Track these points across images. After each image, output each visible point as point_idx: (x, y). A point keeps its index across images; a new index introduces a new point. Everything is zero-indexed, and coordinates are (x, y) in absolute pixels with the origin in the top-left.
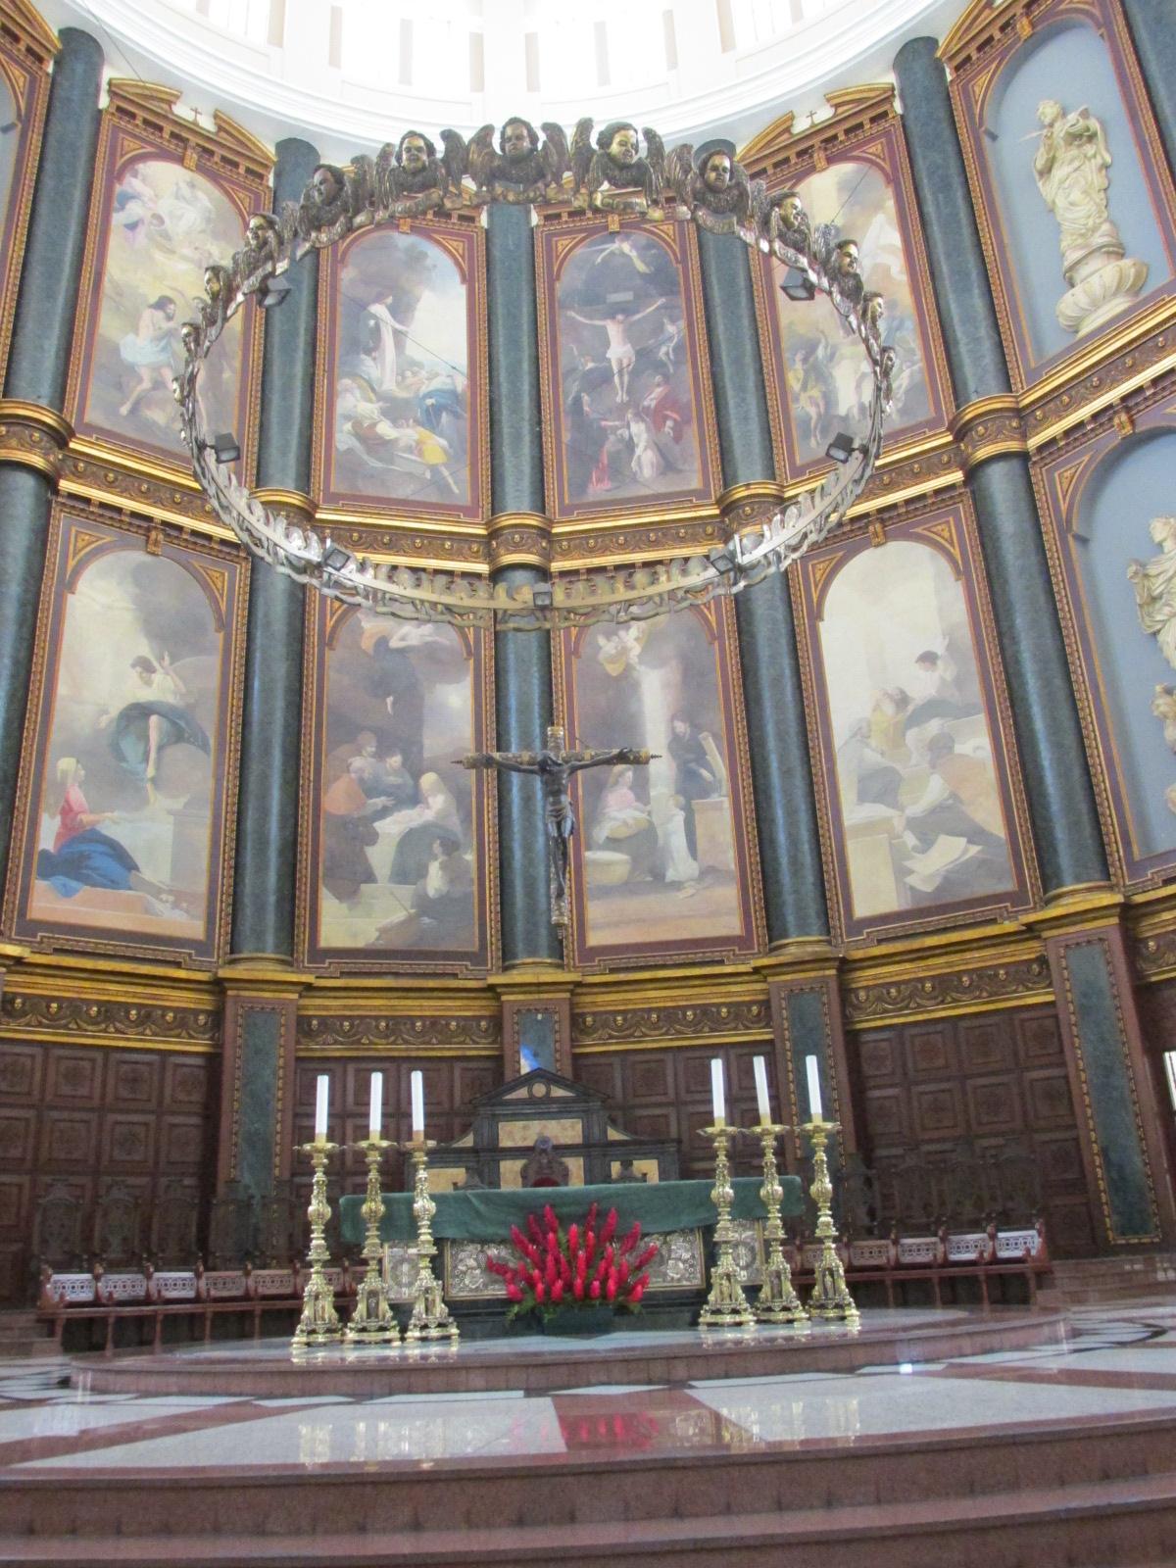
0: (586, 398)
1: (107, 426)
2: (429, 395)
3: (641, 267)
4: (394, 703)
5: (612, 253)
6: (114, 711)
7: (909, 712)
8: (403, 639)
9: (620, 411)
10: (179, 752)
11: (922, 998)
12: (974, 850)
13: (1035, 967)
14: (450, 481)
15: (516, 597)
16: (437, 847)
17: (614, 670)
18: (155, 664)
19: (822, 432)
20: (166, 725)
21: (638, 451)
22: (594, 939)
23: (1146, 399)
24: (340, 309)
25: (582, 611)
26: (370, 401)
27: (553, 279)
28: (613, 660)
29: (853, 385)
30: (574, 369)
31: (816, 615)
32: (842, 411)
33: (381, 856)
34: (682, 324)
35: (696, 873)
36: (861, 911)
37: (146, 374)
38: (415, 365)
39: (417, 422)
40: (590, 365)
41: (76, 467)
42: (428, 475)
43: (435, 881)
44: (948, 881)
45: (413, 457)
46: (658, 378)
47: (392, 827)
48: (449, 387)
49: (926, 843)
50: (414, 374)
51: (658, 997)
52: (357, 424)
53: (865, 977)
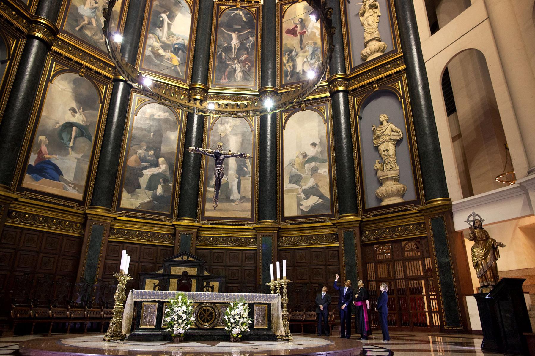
0: (223, 54)
1: (71, 32)
2: (176, 44)
3: (244, 19)
4: (153, 135)
5: (236, 14)
6: (61, 123)
7: (307, 159)
8: (159, 116)
9: (233, 60)
10: (81, 139)
11: (311, 241)
12: (321, 201)
13: (334, 236)
14: (180, 71)
15: (202, 105)
16: (161, 180)
17: (223, 135)
18: (77, 110)
19: (291, 76)
20: (78, 130)
21: (237, 72)
22: (207, 214)
23: (383, 81)
24: (152, 13)
25: (222, 112)
26: (158, 42)
29: (301, 64)
30: (221, 45)
31: (283, 128)
32: (298, 71)
33: (143, 181)
34: (255, 38)
35: (239, 198)
36: (286, 214)
37: (86, 19)
38: (173, 34)
39: (172, 52)
41: (58, 43)
42: (173, 68)
43: (159, 191)
44: (313, 208)
45: (168, 61)
46: (246, 52)
47: (148, 173)
48: (183, 43)
49: (307, 197)
50: (173, 37)
51: (225, 234)
52: (153, 48)
53: (285, 234)
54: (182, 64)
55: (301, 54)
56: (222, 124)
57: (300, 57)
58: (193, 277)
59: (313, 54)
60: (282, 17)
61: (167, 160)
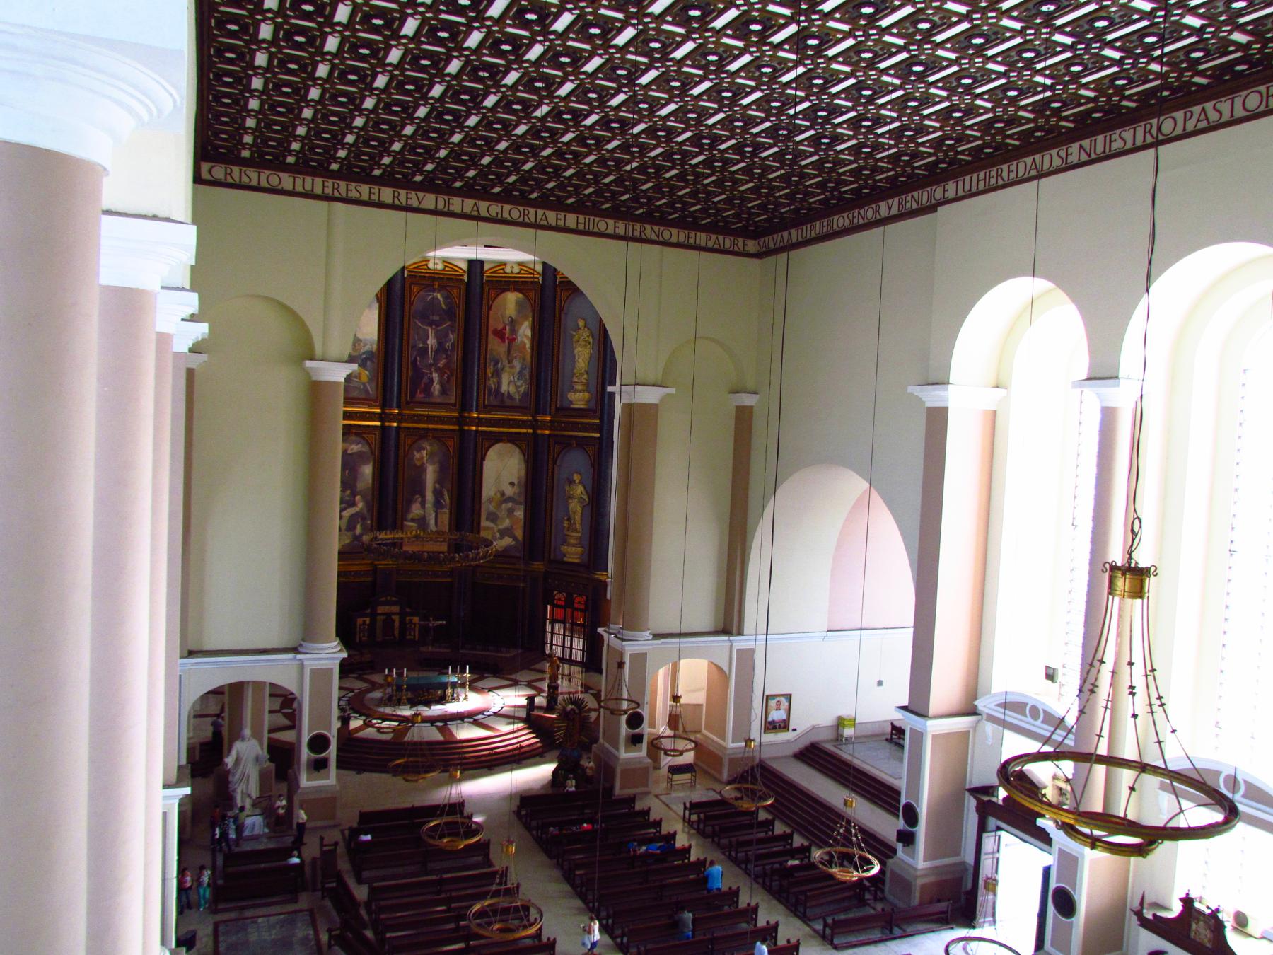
0: (418, 358)
2: (364, 353)
3: (443, 306)
7: (504, 499)
12: (514, 543)
16: (359, 520)
17: (418, 463)
21: (435, 384)
27: (411, 304)
28: (418, 460)
31: (483, 458)
34: (456, 335)
40: (421, 345)
44: (507, 549)
46: (444, 356)
49: (502, 537)
54: (370, 380)
55: (507, 369)
56: (418, 451)
57: (506, 374)
58: (395, 614)
59: (520, 373)
60: (489, 308)
61: (363, 497)
